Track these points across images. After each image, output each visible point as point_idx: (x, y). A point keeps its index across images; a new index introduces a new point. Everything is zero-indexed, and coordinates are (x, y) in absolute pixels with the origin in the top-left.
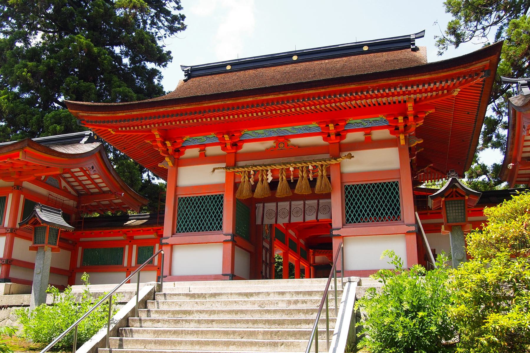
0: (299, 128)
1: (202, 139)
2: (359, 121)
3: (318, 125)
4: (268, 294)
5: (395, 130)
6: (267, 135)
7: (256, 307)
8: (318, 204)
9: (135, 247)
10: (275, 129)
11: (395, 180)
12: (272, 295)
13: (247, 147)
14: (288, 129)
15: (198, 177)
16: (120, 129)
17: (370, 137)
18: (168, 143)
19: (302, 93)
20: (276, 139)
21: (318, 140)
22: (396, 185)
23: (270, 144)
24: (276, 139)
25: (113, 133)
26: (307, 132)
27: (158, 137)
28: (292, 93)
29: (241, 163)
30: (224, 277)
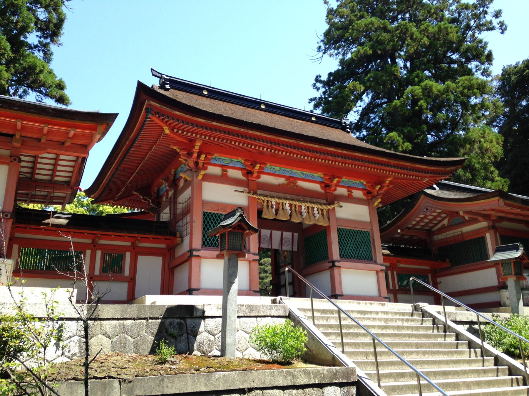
0: (307, 174)
1: (226, 160)
2: (346, 180)
3: (322, 176)
4: (377, 313)
5: (368, 193)
6: (281, 173)
7: (382, 323)
8: (271, 234)
9: (99, 253)
10: (289, 170)
11: (368, 231)
12: (380, 314)
13: (265, 178)
14: (297, 173)
15: (221, 195)
16: (175, 130)
17: (352, 195)
18: (203, 157)
19: (353, 154)
20: (288, 178)
21: (317, 187)
22: (369, 234)
23: (281, 181)
24: (288, 178)
25: (167, 131)
26: (311, 179)
27: (197, 148)
28: (347, 151)
29: (259, 192)
30: (379, 298)
